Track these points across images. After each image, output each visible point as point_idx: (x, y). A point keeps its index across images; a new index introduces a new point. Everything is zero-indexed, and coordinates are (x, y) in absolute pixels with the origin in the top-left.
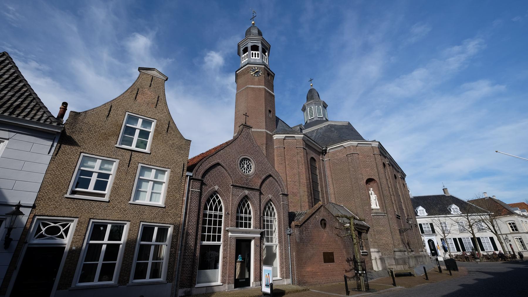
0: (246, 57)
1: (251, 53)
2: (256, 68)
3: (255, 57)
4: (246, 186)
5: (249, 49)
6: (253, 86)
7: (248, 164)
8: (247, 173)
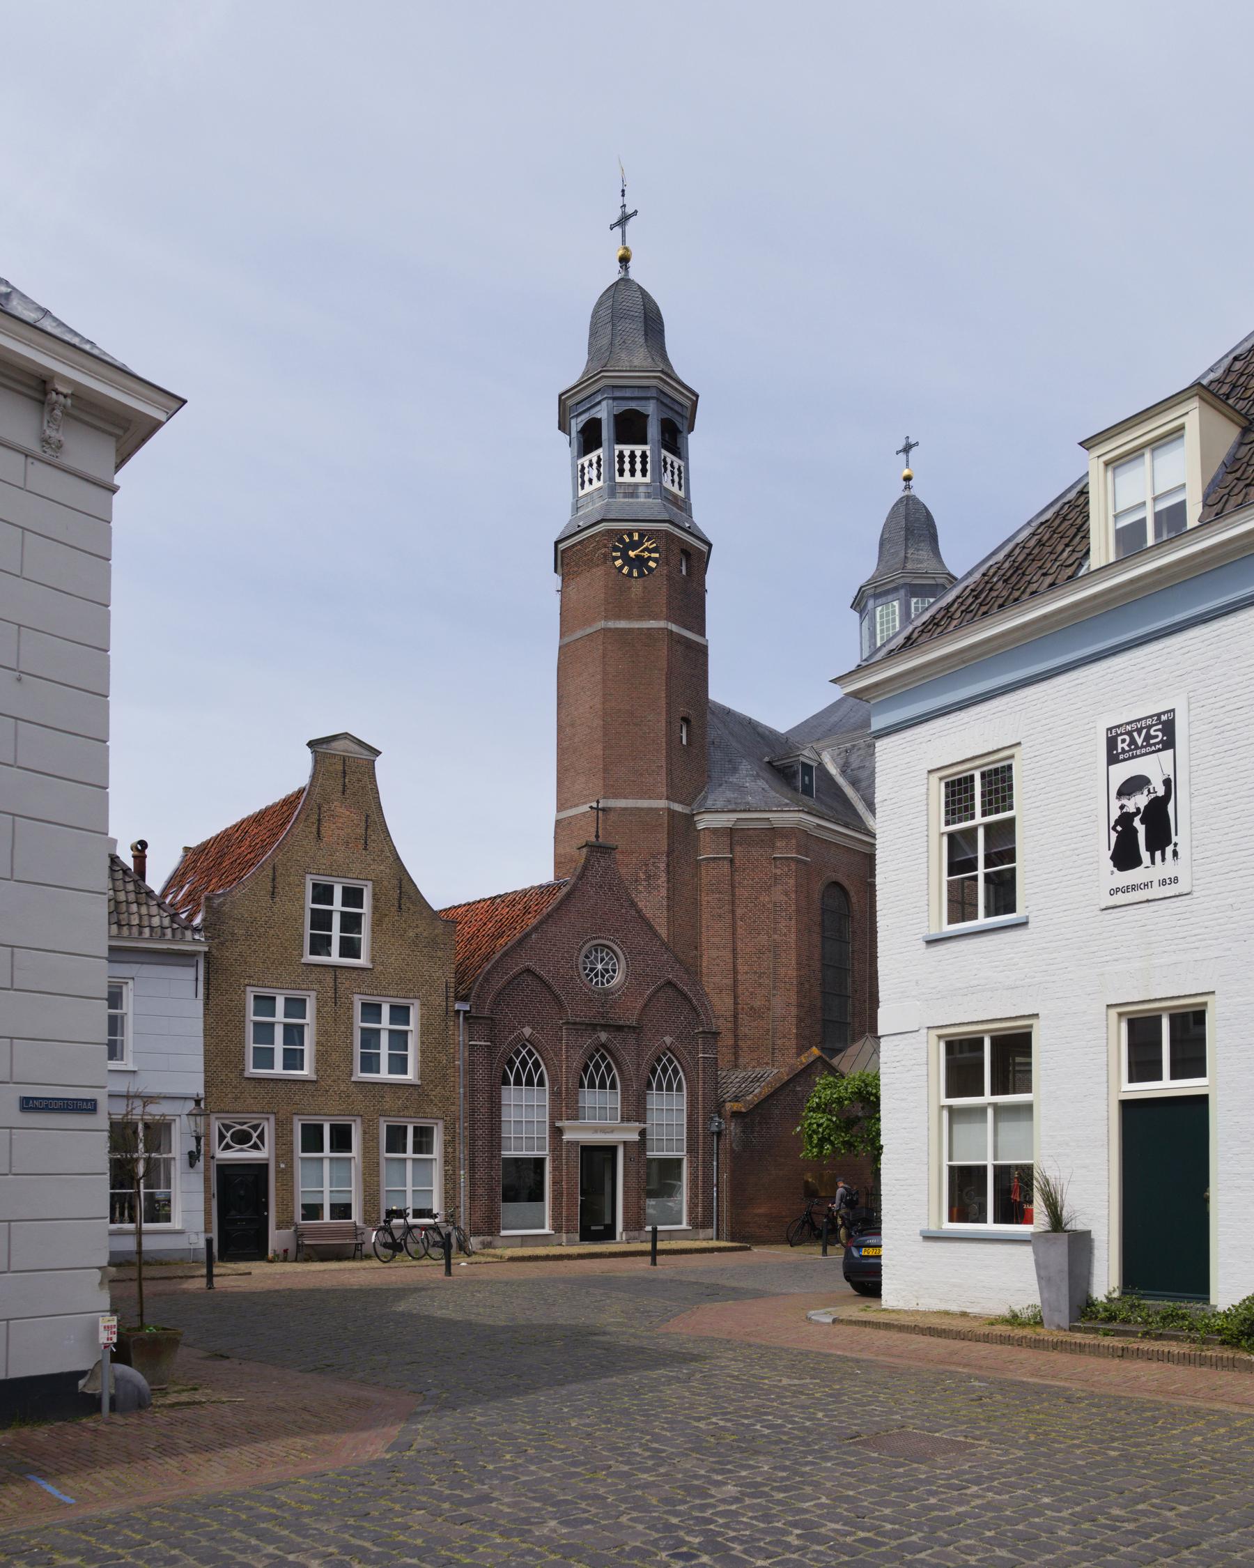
1: (617, 453)
2: (636, 537)
3: (633, 473)
4: (603, 1022)
6: (623, 624)
7: (606, 959)
8: (603, 984)
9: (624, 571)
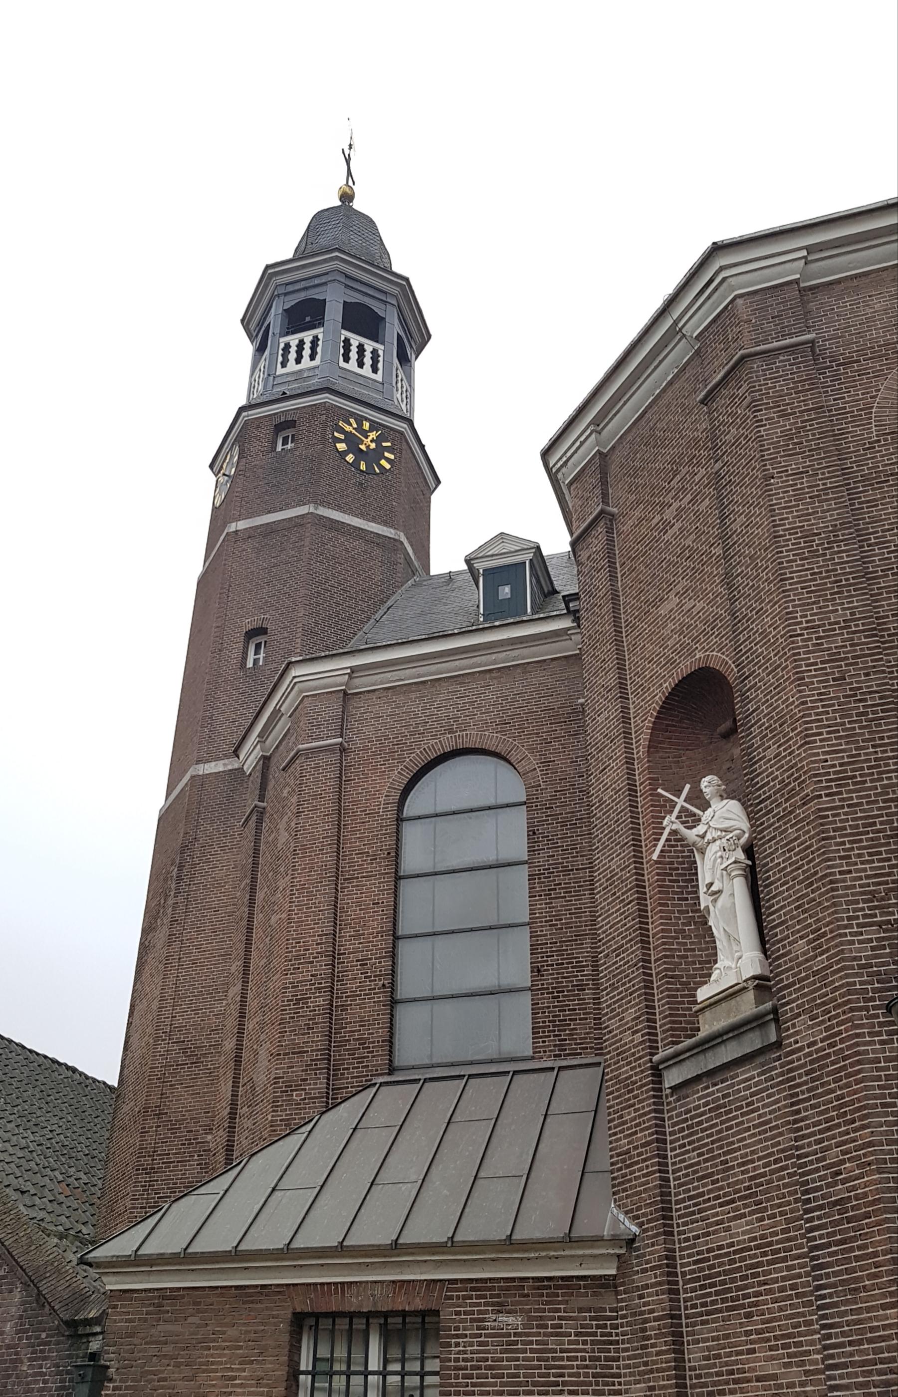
0: (307, 352)
5: (334, 313)
9: (347, 458)
